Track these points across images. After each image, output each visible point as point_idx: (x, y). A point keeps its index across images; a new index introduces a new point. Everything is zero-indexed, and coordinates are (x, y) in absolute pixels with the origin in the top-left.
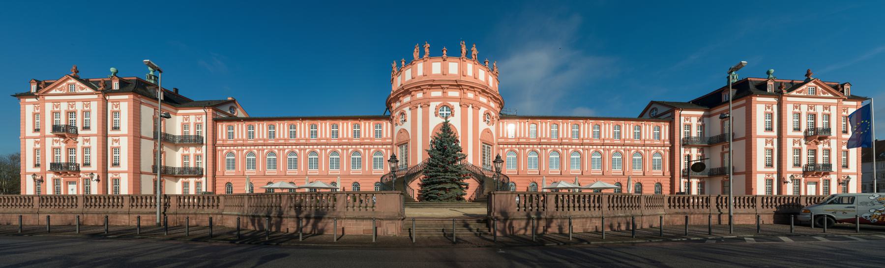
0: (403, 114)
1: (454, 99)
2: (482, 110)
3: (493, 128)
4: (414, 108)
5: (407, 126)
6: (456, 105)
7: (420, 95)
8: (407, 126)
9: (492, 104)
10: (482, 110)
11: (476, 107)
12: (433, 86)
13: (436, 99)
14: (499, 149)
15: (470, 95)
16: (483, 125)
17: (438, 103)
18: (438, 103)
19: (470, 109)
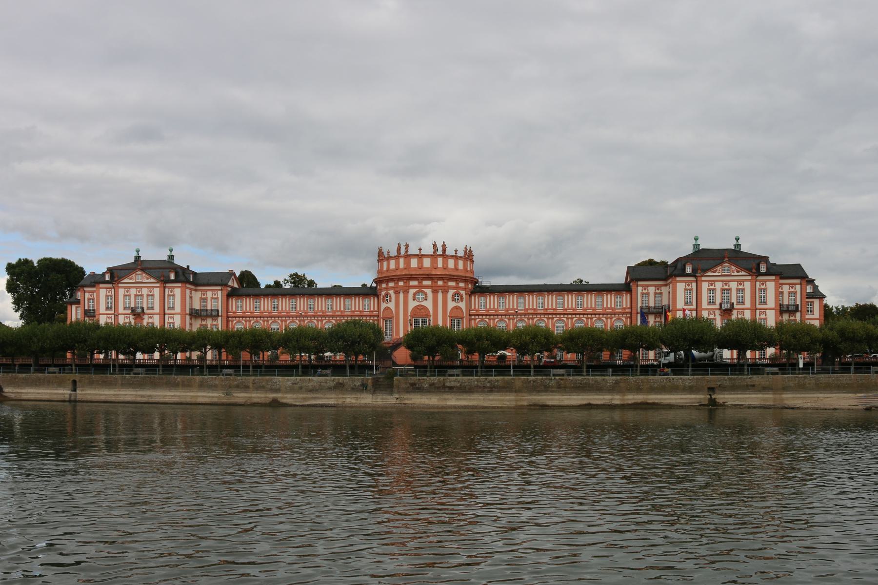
0: (387, 294)
1: (427, 287)
2: (451, 292)
3: (463, 305)
4: (397, 293)
5: (392, 305)
6: (429, 291)
7: (401, 283)
8: (392, 305)
9: (462, 285)
10: (451, 292)
11: (445, 292)
12: (411, 278)
13: (414, 287)
14: (470, 320)
15: (440, 283)
16: (451, 305)
17: (415, 290)
18: (415, 290)
19: (440, 295)
